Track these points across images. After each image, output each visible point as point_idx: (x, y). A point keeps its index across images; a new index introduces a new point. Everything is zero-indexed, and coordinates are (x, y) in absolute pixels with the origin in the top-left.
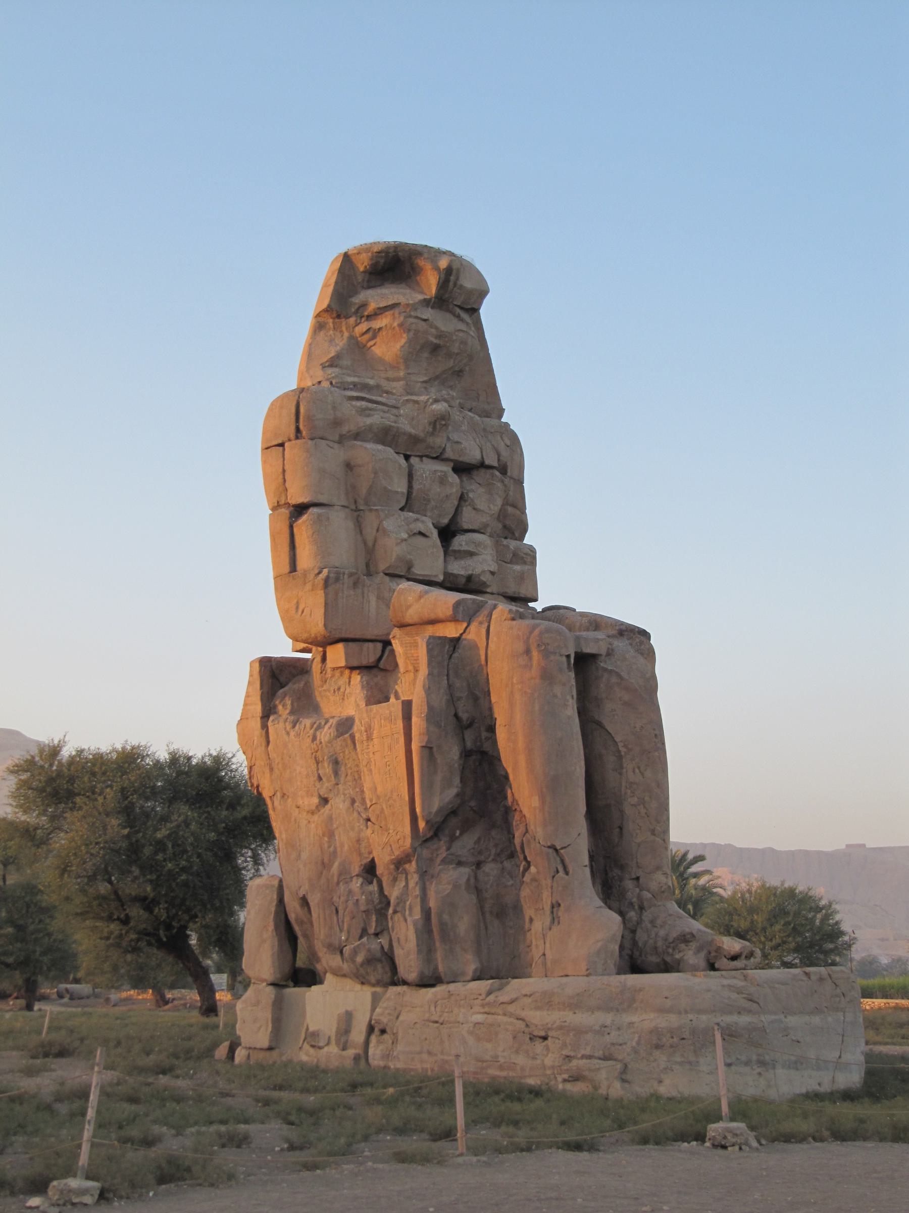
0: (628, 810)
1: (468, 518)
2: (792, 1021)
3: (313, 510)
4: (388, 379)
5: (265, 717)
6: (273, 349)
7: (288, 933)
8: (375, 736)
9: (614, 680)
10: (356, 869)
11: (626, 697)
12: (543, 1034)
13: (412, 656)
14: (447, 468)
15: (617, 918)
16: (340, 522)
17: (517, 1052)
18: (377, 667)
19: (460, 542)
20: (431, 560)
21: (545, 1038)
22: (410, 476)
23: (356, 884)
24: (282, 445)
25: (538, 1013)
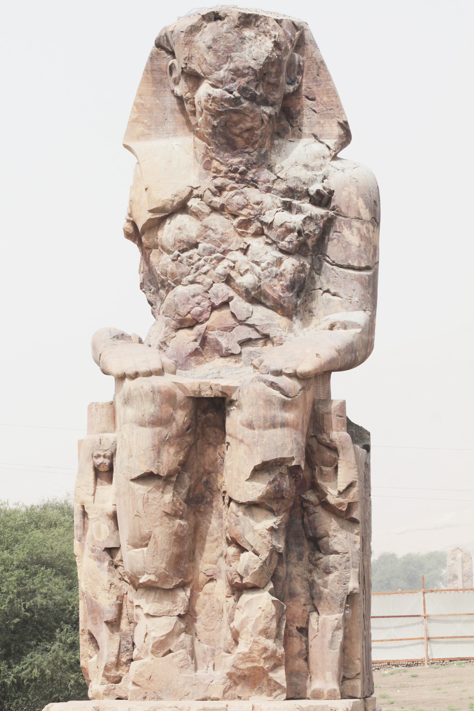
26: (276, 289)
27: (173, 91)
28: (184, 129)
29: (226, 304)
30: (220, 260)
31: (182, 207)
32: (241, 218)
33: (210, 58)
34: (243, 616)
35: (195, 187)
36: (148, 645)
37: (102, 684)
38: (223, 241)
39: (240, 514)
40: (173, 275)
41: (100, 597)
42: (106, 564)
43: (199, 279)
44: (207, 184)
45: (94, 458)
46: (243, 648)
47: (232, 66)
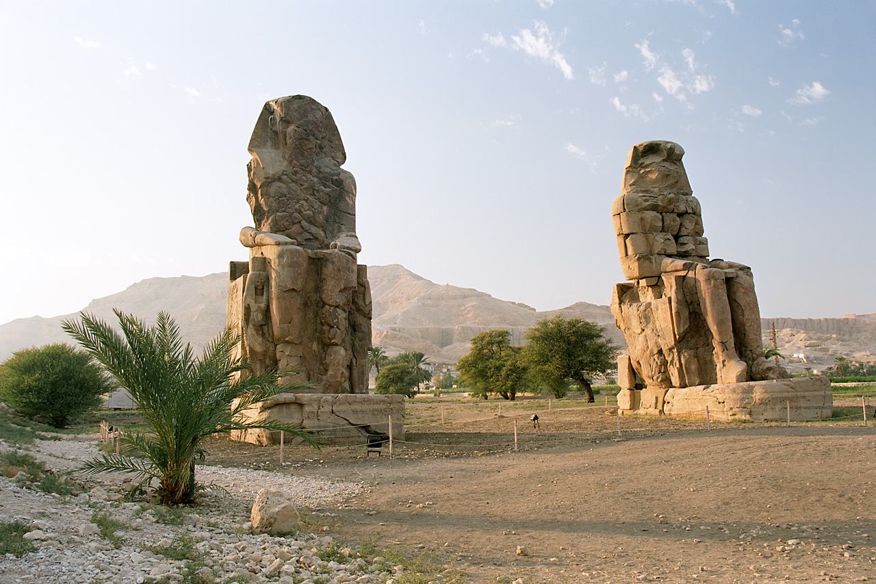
0: (747, 328)
1: (683, 229)
2: (806, 394)
5: (620, 304)
6: (614, 185)
7: (633, 373)
8: (659, 309)
9: (739, 285)
10: (655, 352)
11: (743, 290)
13: (670, 284)
14: (675, 216)
15: (745, 364)
16: (640, 238)
18: (657, 286)
19: (682, 240)
20: (673, 249)
21: (724, 403)
22: (663, 220)
23: (656, 357)
24: (619, 214)
26: (320, 218)
29: (299, 222)
30: (296, 203)
31: (280, 179)
32: (305, 186)
38: (298, 196)
42: (261, 332)
43: (288, 210)
44: (290, 170)
46: (330, 372)
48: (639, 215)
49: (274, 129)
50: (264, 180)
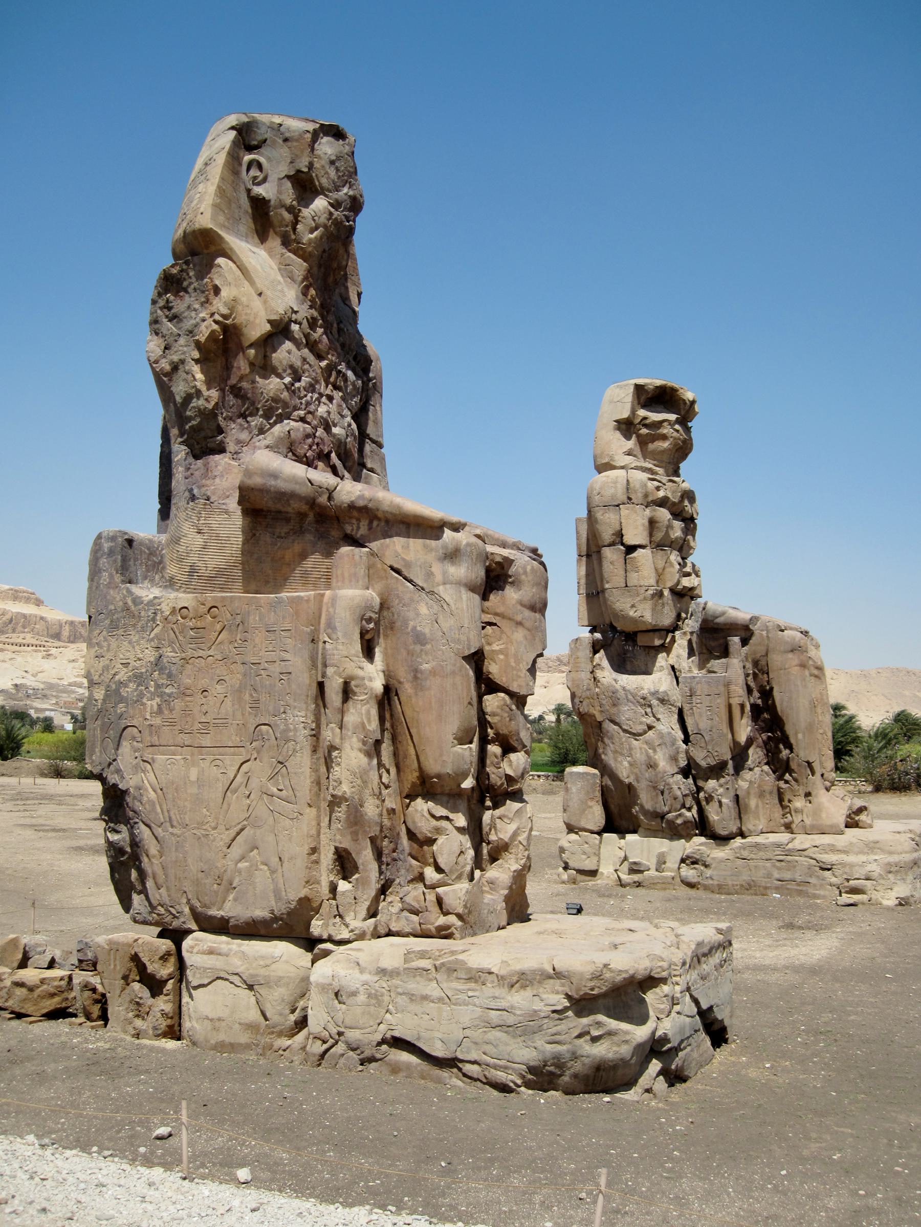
3: (640, 550)
4: (655, 465)
12: (829, 867)
17: (811, 876)
24: (618, 506)
25: (826, 856)
27: (249, 191)
28: (253, 237)
33: (332, 173)
34: (512, 827)
35: (295, 309)
36: (464, 867)
37: (365, 919)
39: (514, 707)
40: (285, 405)
41: (366, 805)
42: (375, 761)
43: (309, 418)
45: (364, 622)
47: (351, 193)
48: (648, 512)
49: (259, 190)
50: (268, 327)
